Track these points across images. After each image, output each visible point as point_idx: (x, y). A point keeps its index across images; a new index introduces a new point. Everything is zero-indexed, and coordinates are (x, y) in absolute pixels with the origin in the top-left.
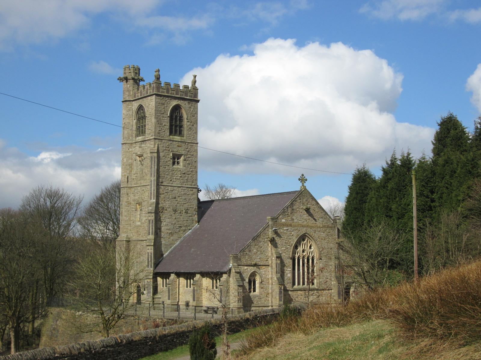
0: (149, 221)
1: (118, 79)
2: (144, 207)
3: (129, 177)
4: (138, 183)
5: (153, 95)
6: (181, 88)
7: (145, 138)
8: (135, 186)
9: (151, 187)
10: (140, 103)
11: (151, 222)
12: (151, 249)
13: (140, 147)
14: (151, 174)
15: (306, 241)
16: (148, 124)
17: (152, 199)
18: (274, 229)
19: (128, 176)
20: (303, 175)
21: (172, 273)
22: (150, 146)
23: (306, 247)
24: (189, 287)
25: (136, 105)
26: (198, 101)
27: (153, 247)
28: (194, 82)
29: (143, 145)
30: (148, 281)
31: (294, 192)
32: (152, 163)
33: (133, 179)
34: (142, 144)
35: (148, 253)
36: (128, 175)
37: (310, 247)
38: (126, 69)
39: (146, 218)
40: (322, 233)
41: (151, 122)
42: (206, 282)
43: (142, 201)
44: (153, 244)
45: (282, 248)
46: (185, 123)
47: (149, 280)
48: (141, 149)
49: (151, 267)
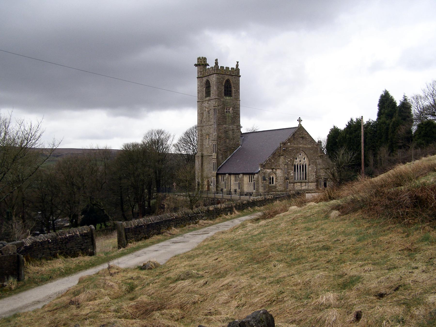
1: (194, 65)
2: (211, 137)
4: (207, 124)
5: (215, 73)
6: (230, 69)
7: (210, 98)
9: (214, 126)
10: (207, 79)
14: (214, 119)
16: (212, 91)
20: (300, 118)
21: (227, 173)
22: (213, 103)
24: (236, 181)
25: (205, 79)
26: (240, 76)
27: (216, 160)
28: (237, 66)
29: (209, 102)
30: (213, 179)
31: (296, 128)
32: (214, 112)
33: (204, 122)
34: (208, 102)
35: (213, 163)
37: (304, 159)
39: (212, 143)
41: (214, 89)
42: (246, 179)
44: (216, 158)
46: (233, 90)
47: (214, 178)
48: (208, 105)
49: (215, 170)
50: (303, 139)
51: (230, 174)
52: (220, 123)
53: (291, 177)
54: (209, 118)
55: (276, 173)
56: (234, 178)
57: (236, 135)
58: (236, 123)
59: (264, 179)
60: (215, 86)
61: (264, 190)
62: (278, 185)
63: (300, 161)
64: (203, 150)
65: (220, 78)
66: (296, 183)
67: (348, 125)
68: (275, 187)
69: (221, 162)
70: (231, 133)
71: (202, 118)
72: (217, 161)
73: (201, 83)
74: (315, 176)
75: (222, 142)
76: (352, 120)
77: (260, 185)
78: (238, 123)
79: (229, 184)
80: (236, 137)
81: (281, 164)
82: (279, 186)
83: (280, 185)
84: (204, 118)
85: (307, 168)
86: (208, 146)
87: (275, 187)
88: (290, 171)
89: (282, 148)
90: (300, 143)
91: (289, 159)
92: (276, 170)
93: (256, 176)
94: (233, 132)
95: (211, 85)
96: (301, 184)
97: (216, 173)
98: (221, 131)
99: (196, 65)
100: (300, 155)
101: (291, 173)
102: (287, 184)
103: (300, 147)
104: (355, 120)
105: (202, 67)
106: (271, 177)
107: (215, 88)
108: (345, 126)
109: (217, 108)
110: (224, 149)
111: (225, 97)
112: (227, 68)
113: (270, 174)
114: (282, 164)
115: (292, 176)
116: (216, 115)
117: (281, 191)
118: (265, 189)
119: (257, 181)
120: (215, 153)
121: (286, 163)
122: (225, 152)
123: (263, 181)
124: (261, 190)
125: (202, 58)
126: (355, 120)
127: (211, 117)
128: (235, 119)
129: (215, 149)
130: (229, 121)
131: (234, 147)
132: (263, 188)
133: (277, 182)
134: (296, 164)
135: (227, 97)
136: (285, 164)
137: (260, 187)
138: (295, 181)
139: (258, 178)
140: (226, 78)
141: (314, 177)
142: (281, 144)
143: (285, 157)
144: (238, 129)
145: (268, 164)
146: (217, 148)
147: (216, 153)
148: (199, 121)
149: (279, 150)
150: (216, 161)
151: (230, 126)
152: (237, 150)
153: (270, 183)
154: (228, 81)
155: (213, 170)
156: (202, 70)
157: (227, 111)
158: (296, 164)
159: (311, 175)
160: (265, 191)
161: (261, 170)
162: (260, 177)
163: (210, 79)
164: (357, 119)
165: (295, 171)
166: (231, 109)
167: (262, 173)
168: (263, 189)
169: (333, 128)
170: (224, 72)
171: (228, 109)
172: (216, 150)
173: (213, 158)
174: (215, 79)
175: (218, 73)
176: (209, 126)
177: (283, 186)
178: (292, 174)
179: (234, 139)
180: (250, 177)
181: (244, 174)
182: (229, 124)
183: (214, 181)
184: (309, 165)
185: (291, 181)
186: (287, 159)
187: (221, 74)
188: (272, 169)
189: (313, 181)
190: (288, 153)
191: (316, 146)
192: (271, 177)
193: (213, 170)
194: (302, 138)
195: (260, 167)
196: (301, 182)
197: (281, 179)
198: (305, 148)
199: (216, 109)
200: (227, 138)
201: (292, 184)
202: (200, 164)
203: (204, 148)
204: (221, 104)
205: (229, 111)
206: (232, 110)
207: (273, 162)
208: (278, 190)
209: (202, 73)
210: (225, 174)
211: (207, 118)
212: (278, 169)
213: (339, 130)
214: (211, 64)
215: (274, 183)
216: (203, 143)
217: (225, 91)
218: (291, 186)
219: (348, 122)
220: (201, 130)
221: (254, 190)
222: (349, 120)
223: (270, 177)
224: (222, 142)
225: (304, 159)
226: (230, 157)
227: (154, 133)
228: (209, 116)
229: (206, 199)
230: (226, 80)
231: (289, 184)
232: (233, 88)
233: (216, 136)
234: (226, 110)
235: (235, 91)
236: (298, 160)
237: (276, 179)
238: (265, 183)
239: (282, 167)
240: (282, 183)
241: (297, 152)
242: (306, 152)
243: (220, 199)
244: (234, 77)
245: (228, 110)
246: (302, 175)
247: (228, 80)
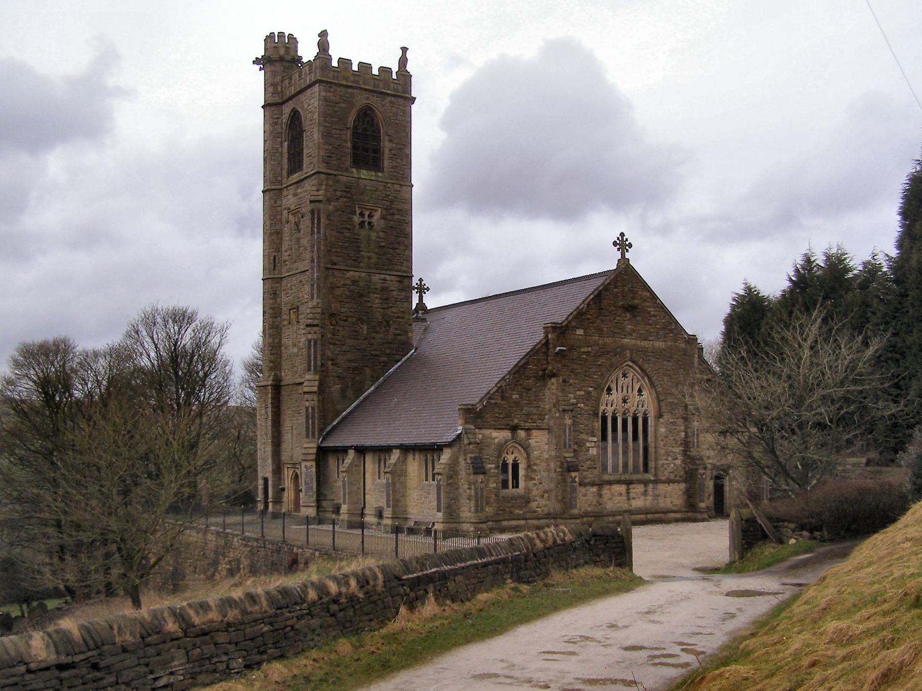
0: (309, 341)
1: (254, 62)
3: (277, 258)
7: (302, 175)
8: (287, 274)
9: (313, 273)
10: (293, 106)
11: (312, 344)
12: (313, 400)
13: (295, 195)
15: (630, 379)
17: (315, 296)
18: (558, 348)
19: (275, 257)
20: (622, 234)
23: (630, 390)
25: (287, 109)
26: (413, 100)
27: (315, 397)
29: (299, 190)
30: (306, 467)
32: (313, 223)
33: (285, 261)
35: (307, 408)
36: (275, 254)
37: (640, 391)
38: (269, 40)
40: (665, 363)
42: (414, 466)
43: (299, 303)
44: (315, 389)
45: (578, 393)
46: (386, 146)
47: (308, 464)
50: (634, 316)
52: (334, 264)
53: (587, 460)
55: (529, 445)
56: (377, 465)
57: (394, 310)
58: (396, 267)
59: (478, 468)
60: (316, 130)
61: (476, 511)
62: (535, 492)
63: (625, 401)
64: (280, 363)
65: (337, 99)
66: (610, 483)
67: (794, 279)
68: (526, 500)
69: (339, 407)
70: (376, 300)
71: (279, 250)
72: (322, 402)
73: (276, 123)
74: (680, 457)
75: (341, 333)
76: (808, 261)
77: (461, 490)
78: (404, 268)
79: (359, 488)
80: (398, 317)
81: (550, 411)
82: (542, 496)
83: (545, 492)
84: (284, 249)
85: (651, 429)
86: (295, 350)
87: (526, 500)
88: (584, 436)
89: (551, 346)
90: (623, 329)
91: (583, 393)
92: (529, 436)
93: (446, 456)
94: (387, 299)
95: (306, 124)
96: (628, 489)
97: (314, 445)
98: (338, 292)
99: (256, 61)
100: (624, 376)
101: (588, 444)
102: (574, 490)
103: (624, 348)
104: (820, 260)
105: (278, 67)
106: (510, 462)
107: (316, 136)
108: (786, 285)
109: (321, 206)
110: (350, 361)
111: (354, 170)
112: (365, 67)
113: (501, 448)
114: (554, 410)
115: (592, 459)
116: (319, 232)
117: (549, 514)
118: (482, 510)
119: (451, 477)
120: (312, 372)
121: (567, 408)
122: (355, 369)
123: (472, 477)
124: (467, 512)
125: (281, 35)
126: (820, 260)
127: (305, 242)
128: (391, 251)
129: (315, 358)
130: (369, 258)
131: (388, 351)
132: (473, 503)
133: (534, 479)
134: (610, 410)
135: (365, 172)
136: (564, 411)
137: (464, 501)
138: (606, 477)
139: (453, 466)
140: (361, 100)
141: (678, 462)
142: (546, 334)
143: (564, 381)
144: (403, 290)
145: (497, 410)
146: (323, 355)
147: (315, 373)
149: (541, 356)
150: (316, 403)
151: (376, 278)
152: (399, 363)
153: (505, 484)
154: (366, 114)
155: (307, 436)
156: (279, 78)
157: (363, 222)
158: (610, 410)
159: (668, 454)
160: (480, 514)
161: (466, 431)
162: (461, 460)
163: (302, 108)
164: (828, 257)
165: (604, 438)
166: (377, 215)
167: (469, 444)
168: (473, 509)
169: (742, 292)
170: (352, 79)
171: (367, 213)
172: (319, 363)
173: (306, 389)
174: (316, 104)
175: (331, 83)
177: (557, 496)
178: (593, 452)
179: (388, 325)
180: (426, 461)
182: (370, 268)
184: (660, 415)
185: (590, 476)
186: (572, 390)
187: (341, 85)
188: (514, 429)
189: (672, 476)
190: (575, 366)
191: (683, 345)
192: (510, 462)
194: (631, 309)
195: (460, 422)
196: (629, 483)
197: (548, 470)
198: (644, 351)
199: (319, 212)
200: (363, 322)
201: (594, 489)
202: (270, 413)
203: (284, 355)
204: (338, 193)
205: (370, 223)
206: (383, 217)
207: (517, 403)
208: (535, 512)
209: (279, 90)
211: (291, 249)
212: (539, 428)
213: (763, 299)
214: (307, 51)
215: (522, 483)
216: (280, 340)
217: (355, 148)
218: (590, 497)
219: (797, 270)
221: (439, 510)
222: (800, 261)
223: (504, 461)
224: (341, 333)
225: (640, 391)
226: (372, 388)
227: (159, 320)
229: (255, 544)
230: (361, 110)
231: (583, 490)
232: (387, 138)
233: (319, 310)
234: (357, 219)
235: (393, 152)
236: (616, 396)
237: (529, 467)
238: (483, 485)
239: (552, 423)
240: (552, 486)
241: (612, 367)
242: (646, 366)
243: (299, 547)
244: (391, 102)
245: (366, 218)
246: (631, 454)
247: (369, 112)
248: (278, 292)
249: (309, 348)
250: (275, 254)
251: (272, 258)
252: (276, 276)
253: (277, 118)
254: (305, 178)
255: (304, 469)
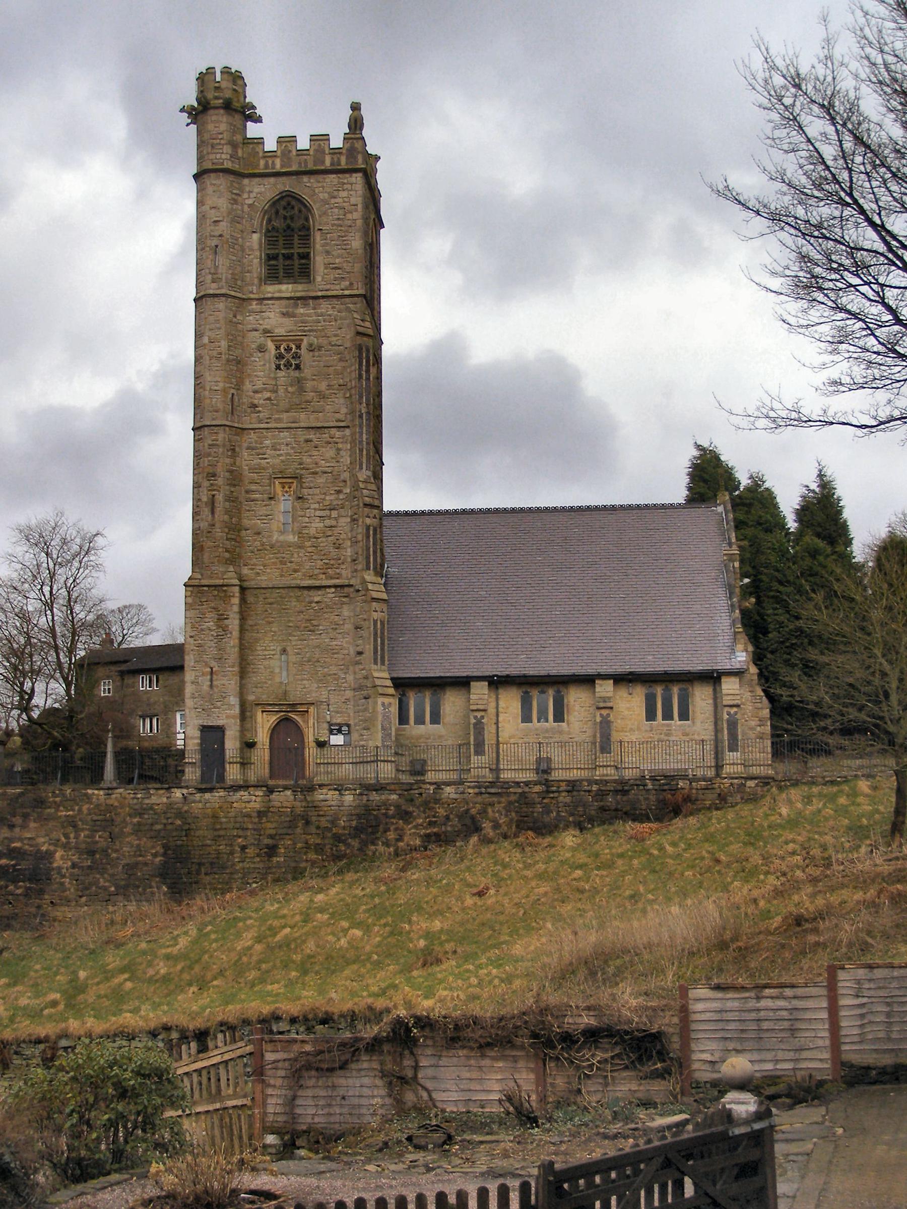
3: (236, 398)
9: (361, 434)
11: (371, 532)
14: (361, 397)
17: (364, 466)
19: (233, 394)
28: (356, 124)
30: (383, 704)
34: (296, 306)
35: (375, 622)
36: (233, 391)
47: (387, 700)
48: (287, 321)
51: (497, 682)
54: (302, 390)
71: (239, 386)
73: (235, 202)
116: (368, 379)
120: (371, 572)
148: (226, 397)
176: (300, 432)
181: (497, 682)
183: (386, 717)
193: (376, 663)
199: (368, 351)
210: (463, 683)
216: (240, 519)
220: (234, 450)
228: (299, 381)
248: (237, 449)
249: (368, 537)
250: (233, 391)
251: (230, 396)
252: (236, 425)
253: (236, 194)
254: (323, 297)
255: (380, 708)
